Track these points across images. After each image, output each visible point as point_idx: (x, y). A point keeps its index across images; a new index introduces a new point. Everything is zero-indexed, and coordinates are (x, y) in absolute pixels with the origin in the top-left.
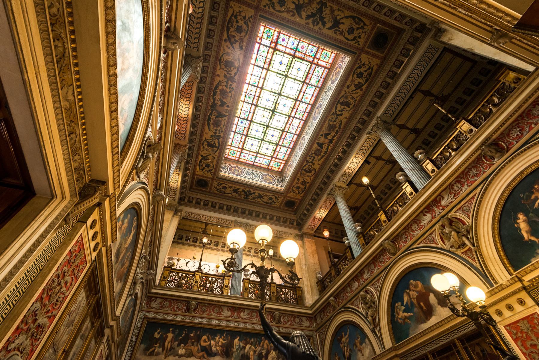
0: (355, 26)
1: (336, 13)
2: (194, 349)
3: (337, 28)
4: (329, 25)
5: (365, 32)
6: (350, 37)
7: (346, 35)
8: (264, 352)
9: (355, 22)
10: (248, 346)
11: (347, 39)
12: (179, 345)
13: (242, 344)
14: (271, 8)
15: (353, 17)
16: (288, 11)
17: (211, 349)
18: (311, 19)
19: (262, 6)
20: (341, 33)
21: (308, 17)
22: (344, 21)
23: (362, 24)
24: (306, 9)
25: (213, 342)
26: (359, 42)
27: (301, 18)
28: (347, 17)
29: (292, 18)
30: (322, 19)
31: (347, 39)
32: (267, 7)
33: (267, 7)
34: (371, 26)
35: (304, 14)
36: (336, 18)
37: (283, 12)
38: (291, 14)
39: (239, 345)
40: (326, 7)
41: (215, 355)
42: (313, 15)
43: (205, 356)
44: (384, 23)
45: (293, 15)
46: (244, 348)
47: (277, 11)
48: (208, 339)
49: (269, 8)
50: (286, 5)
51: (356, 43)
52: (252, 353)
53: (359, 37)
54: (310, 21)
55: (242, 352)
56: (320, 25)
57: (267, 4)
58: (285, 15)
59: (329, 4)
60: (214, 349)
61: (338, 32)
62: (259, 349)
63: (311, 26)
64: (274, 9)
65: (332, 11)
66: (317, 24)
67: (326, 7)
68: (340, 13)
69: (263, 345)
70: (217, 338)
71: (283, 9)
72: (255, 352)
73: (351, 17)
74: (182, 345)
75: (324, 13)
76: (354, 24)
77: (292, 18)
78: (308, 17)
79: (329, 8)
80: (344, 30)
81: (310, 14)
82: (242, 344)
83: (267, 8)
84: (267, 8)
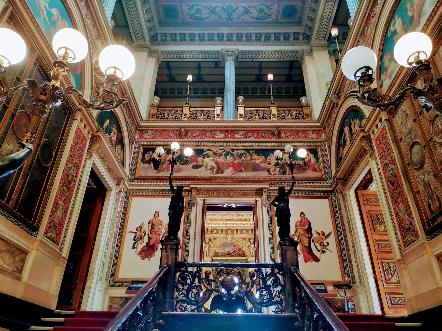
0: (197, 15)
1: (217, 18)
3: (211, 9)
4: (218, 9)
5: (187, 14)
6: (197, 7)
7: (200, 8)
9: (199, 17)
11: (198, 5)
14: (269, 5)
15: (202, 19)
16: (254, 7)
18: (234, 8)
19: (276, 4)
20: (205, 8)
21: (237, 8)
22: (208, 15)
23: (193, 17)
24: (241, 12)
26: (188, 6)
27: (243, 7)
28: (207, 18)
29: (249, 4)
30: (226, 11)
31: (198, 5)
32: (272, 4)
33: (272, 4)
34: (185, 19)
35: (241, 9)
36: (215, 15)
37: (258, 5)
38: (251, 6)
40: (226, 19)
42: (234, 11)
44: (177, 25)
45: (250, 6)
47: (263, 4)
49: (270, 4)
50: (258, 10)
51: (189, 5)
53: (189, 9)
54: (234, 7)
56: (225, 7)
57: (272, 6)
58: (256, 4)
59: (226, 20)
61: (208, 7)
63: (232, 4)
64: (265, 5)
65: (220, 17)
66: (228, 7)
67: (226, 19)
68: (215, 18)
71: (259, 7)
73: (204, 19)
75: (226, 15)
76: (199, 16)
77: (249, 4)
78: (237, 8)
79: (224, 19)
80: (204, 10)
81: (237, 11)
83: (272, 4)
84: (272, 4)
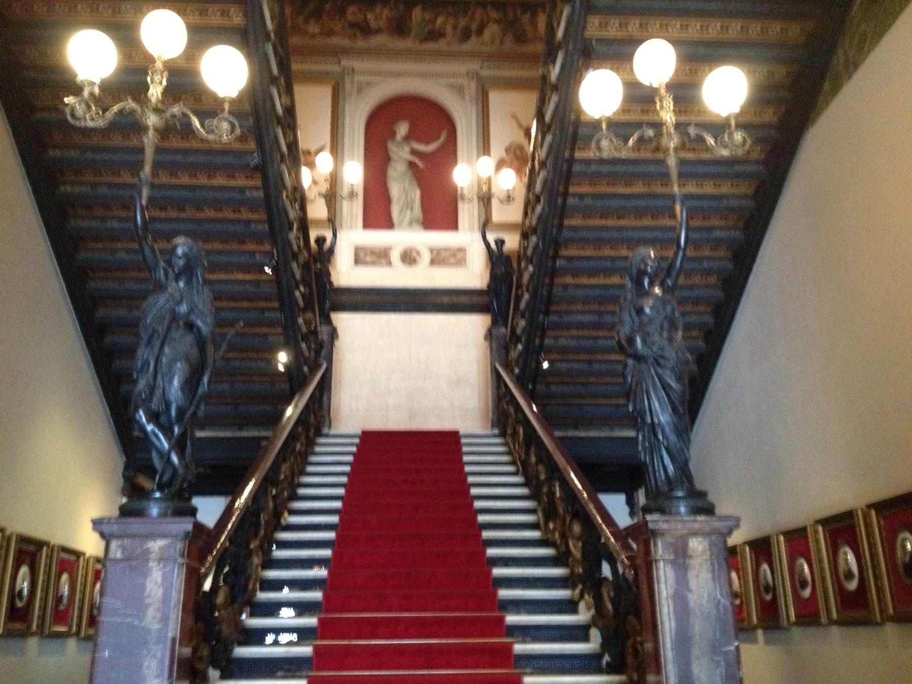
2: (338, 27)
8: (474, 27)
10: (440, 20)
12: (307, 20)
13: (427, 17)
17: (368, 24)
25: (370, 16)
39: (423, 19)
41: (377, 32)
43: (358, 34)
46: (434, 22)
48: (360, 10)
52: (449, 28)
55: (428, 28)
60: (373, 24)
62: (462, 23)
69: (472, 18)
70: (378, 10)
72: (455, 27)
74: (312, 21)
82: (427, 17)
